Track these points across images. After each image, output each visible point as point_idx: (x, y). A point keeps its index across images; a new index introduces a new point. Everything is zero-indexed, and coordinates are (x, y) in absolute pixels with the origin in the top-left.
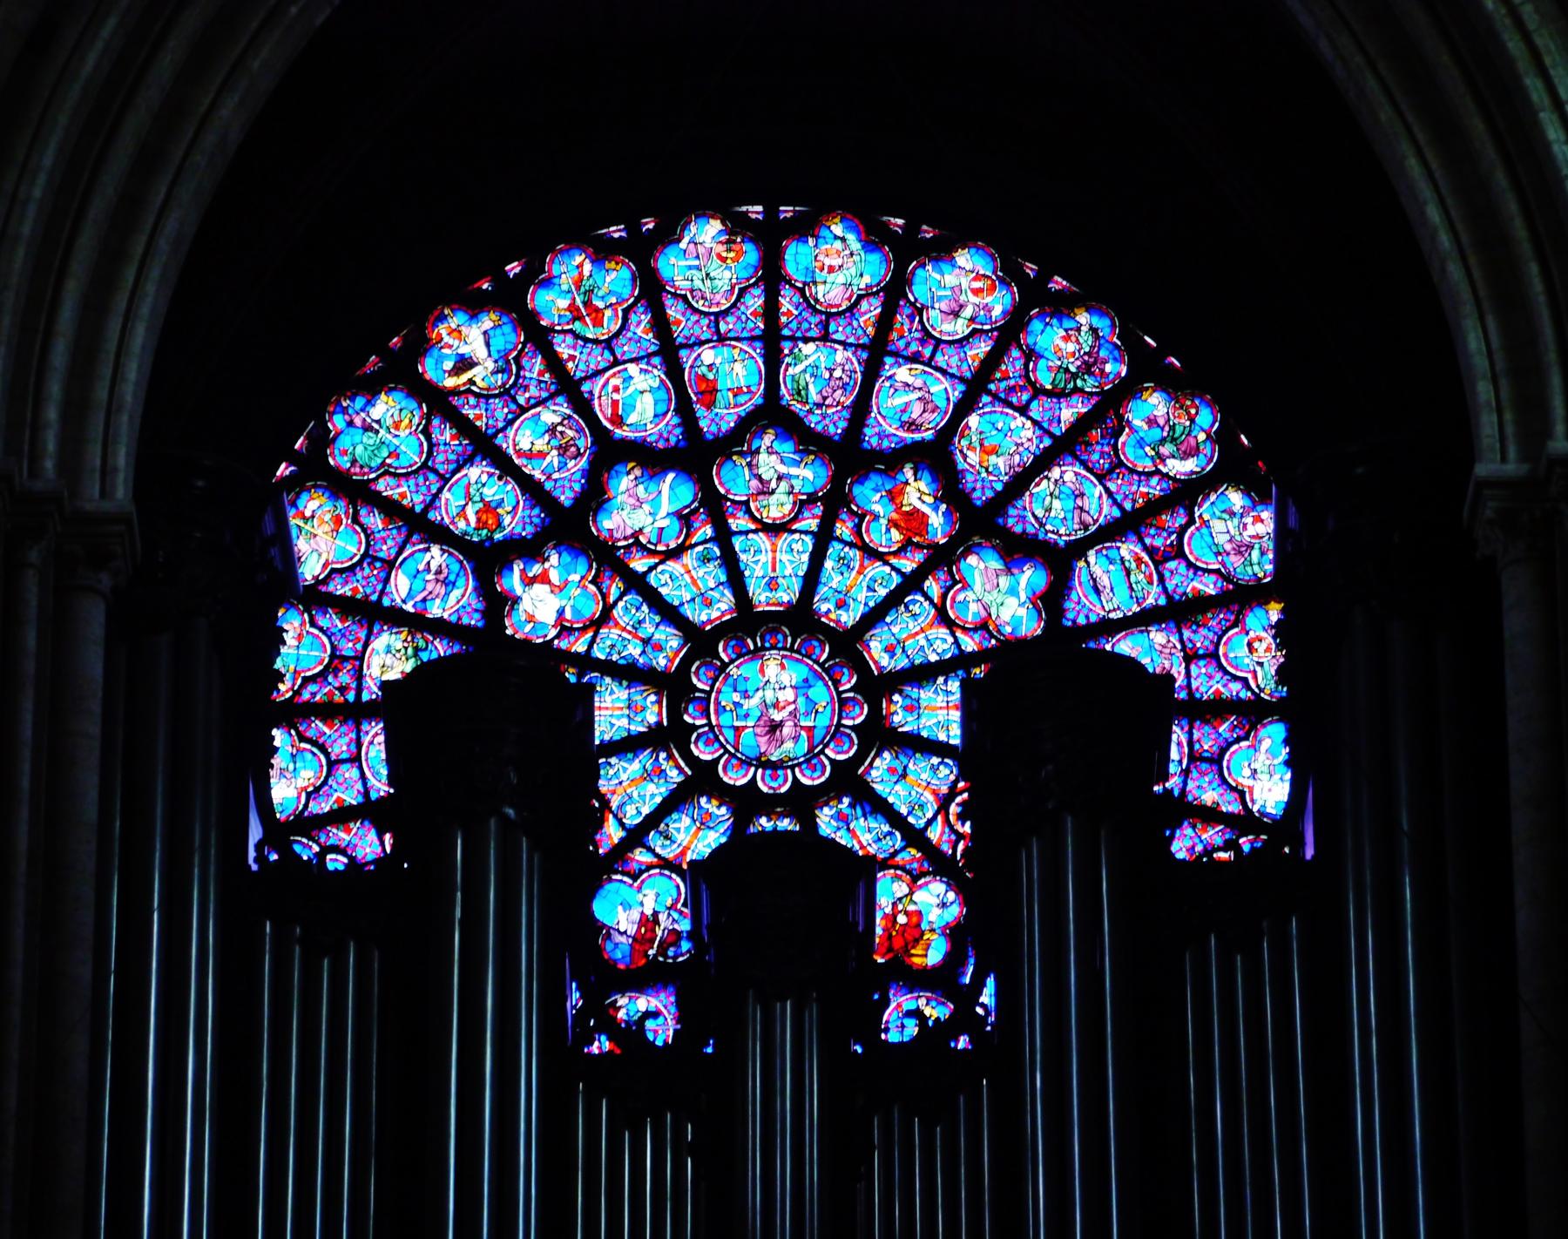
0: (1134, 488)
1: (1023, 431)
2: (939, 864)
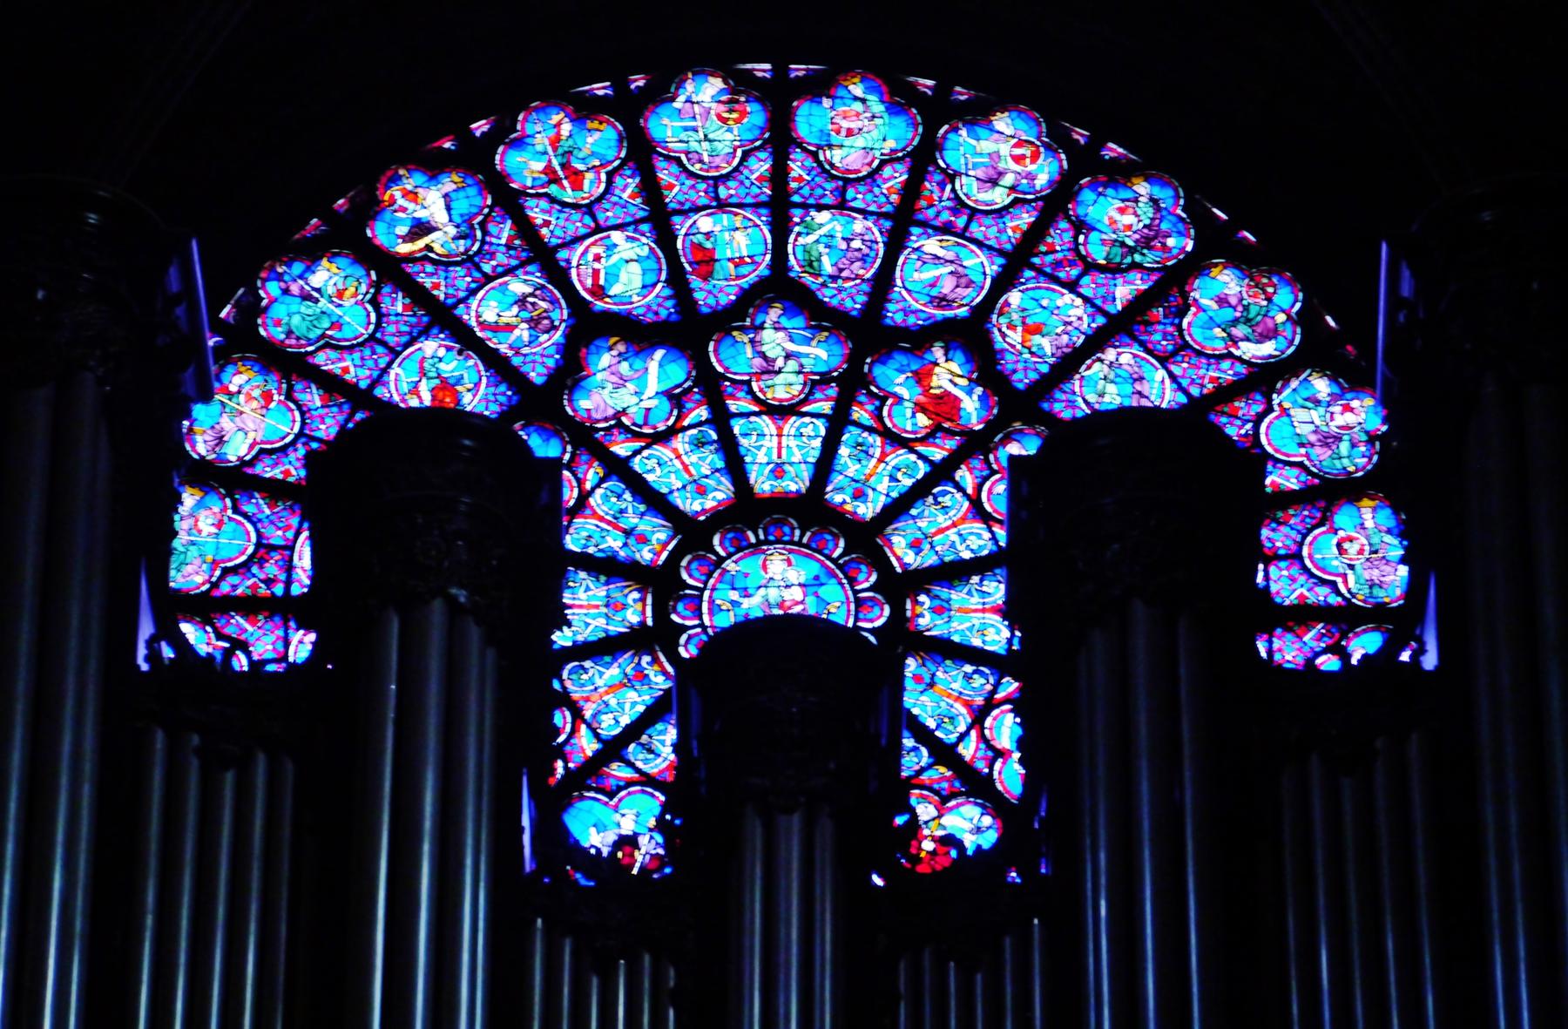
0: (1202, 372)
1: (1072, 307)
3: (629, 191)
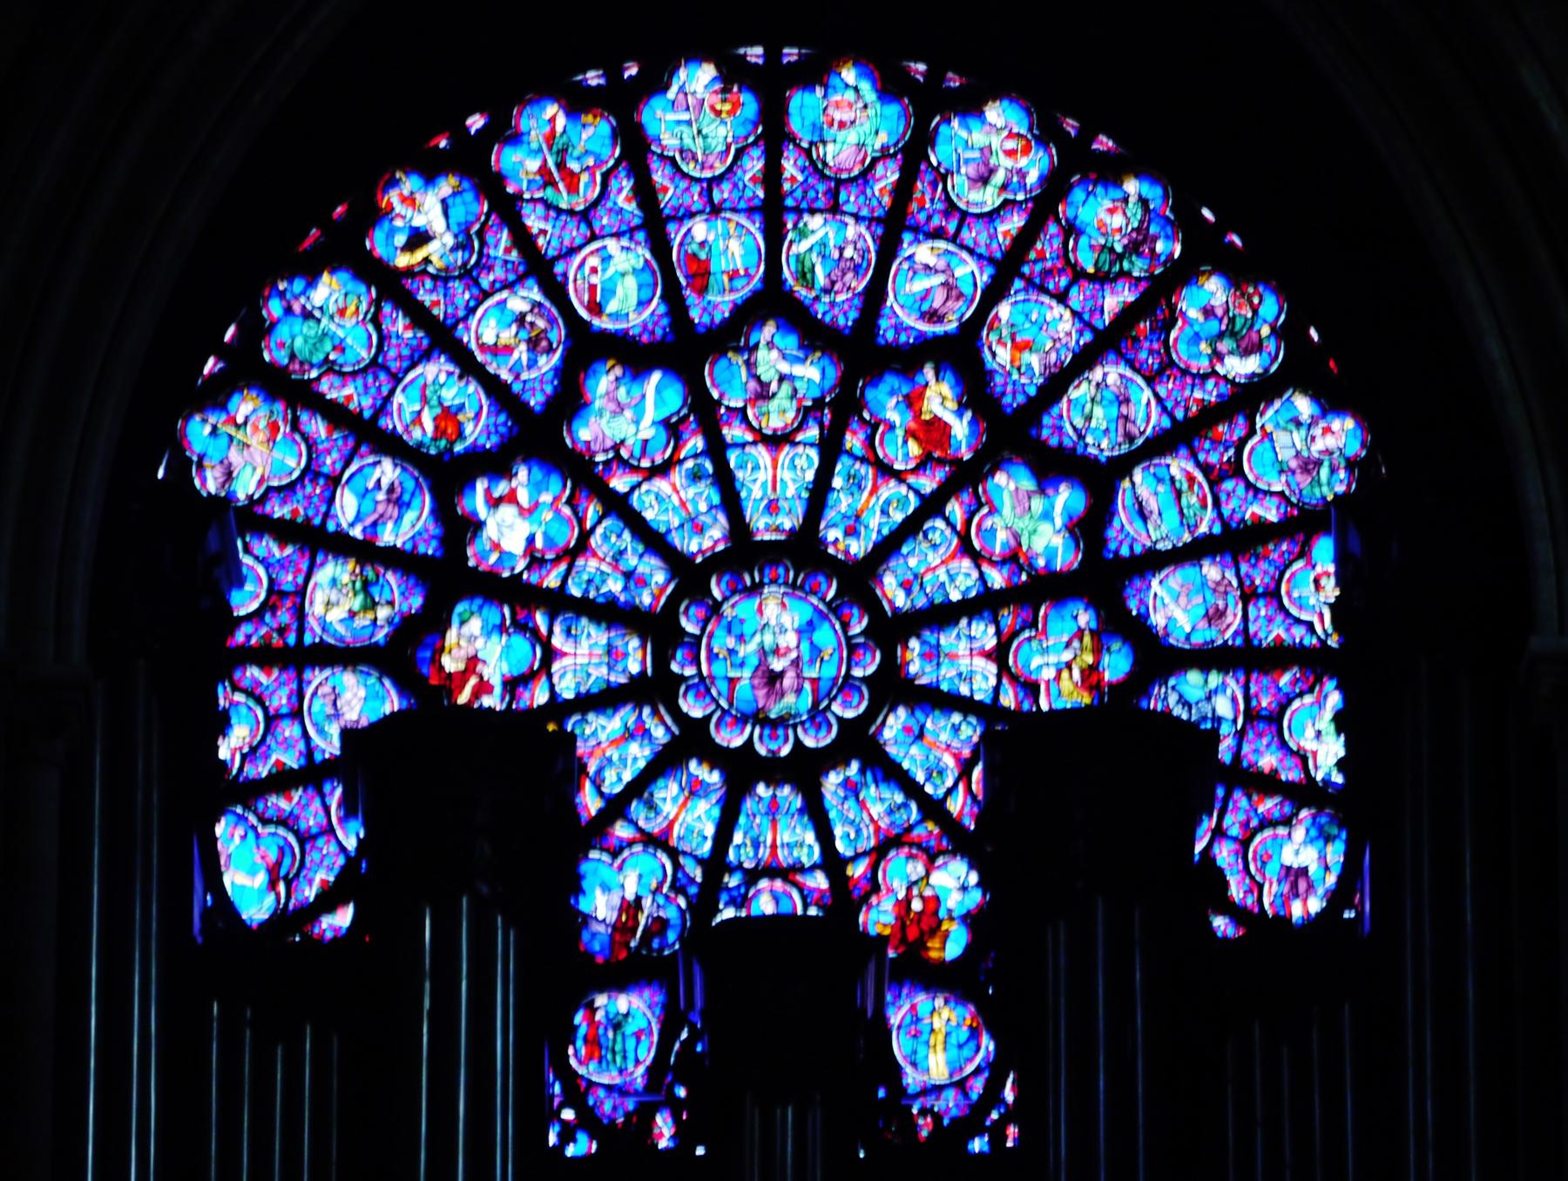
0: (1187, 393)
2: (958, 841)
3: (624, 193)
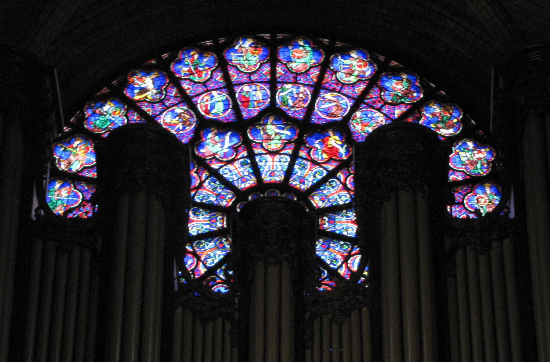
3: (219, 77)
